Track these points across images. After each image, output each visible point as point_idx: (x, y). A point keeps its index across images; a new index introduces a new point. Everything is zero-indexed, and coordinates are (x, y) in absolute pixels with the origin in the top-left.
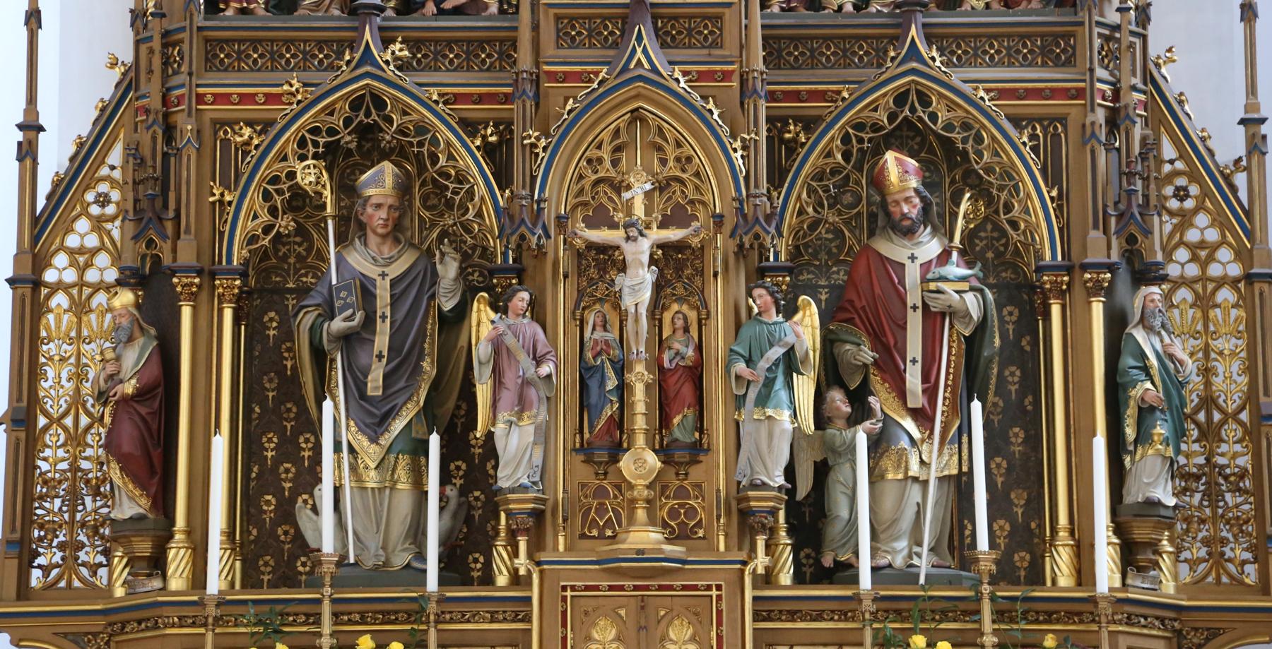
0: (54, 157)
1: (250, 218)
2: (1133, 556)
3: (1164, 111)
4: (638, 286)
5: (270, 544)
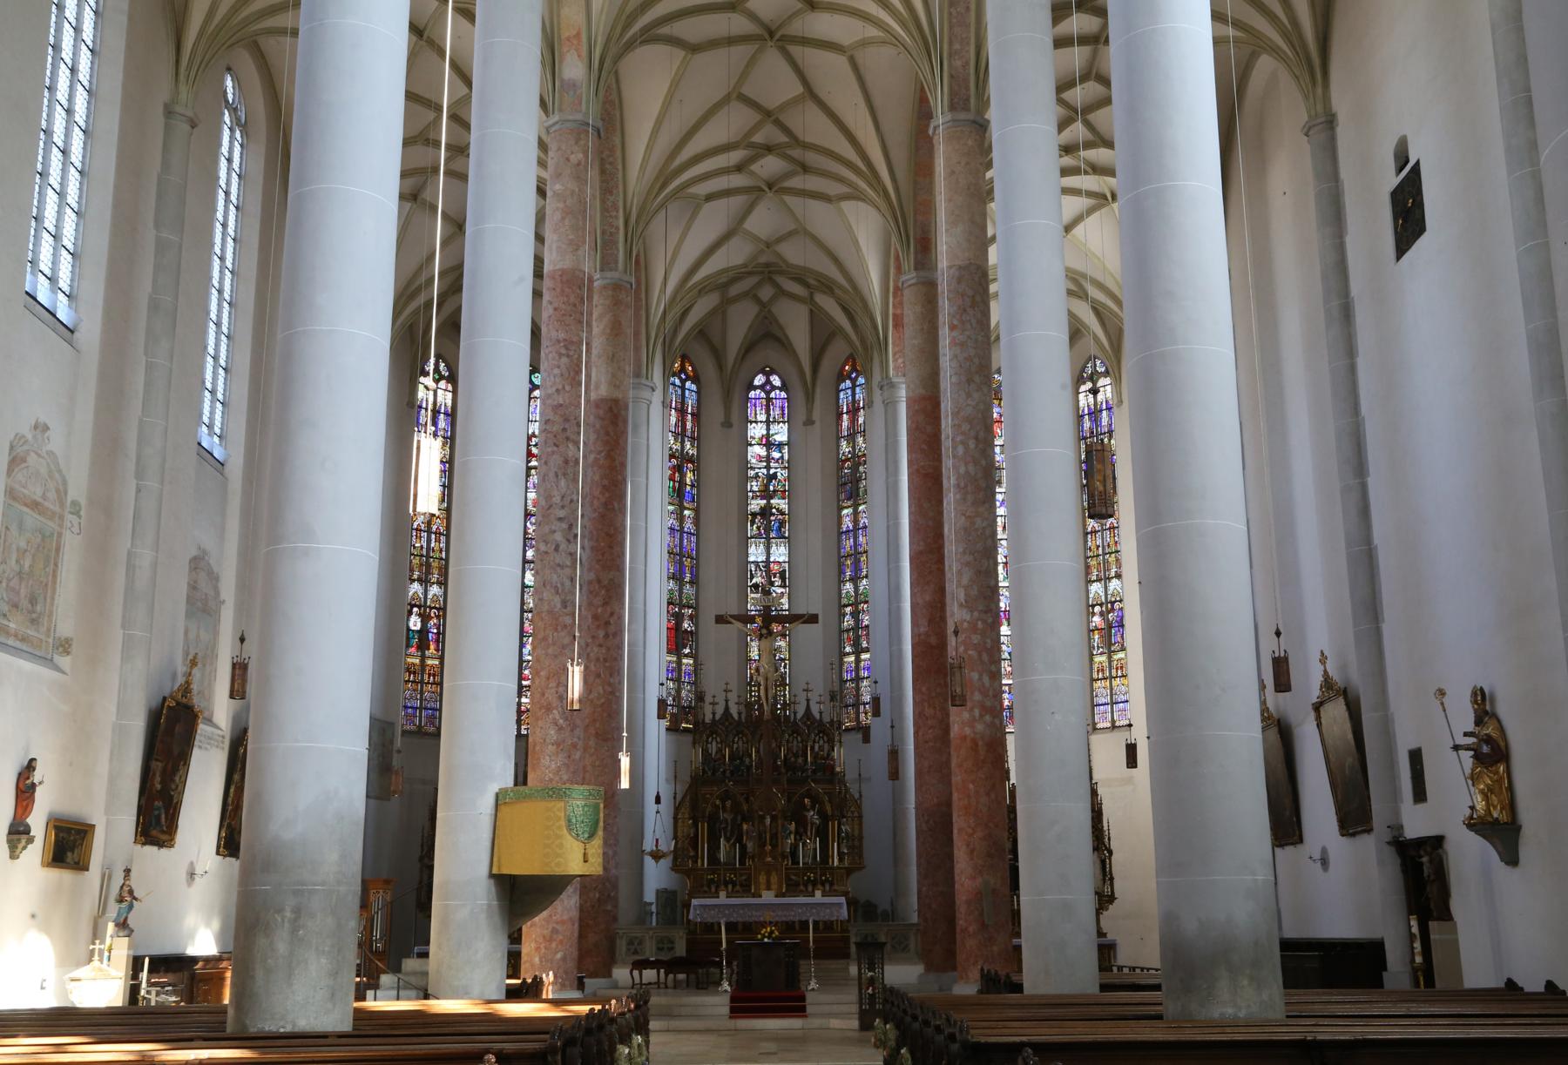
0: (679, 798)
1: (709, 809)
2: (841, 860)
3: (847, 790)
4: (768, 821)
5: (713, 859)
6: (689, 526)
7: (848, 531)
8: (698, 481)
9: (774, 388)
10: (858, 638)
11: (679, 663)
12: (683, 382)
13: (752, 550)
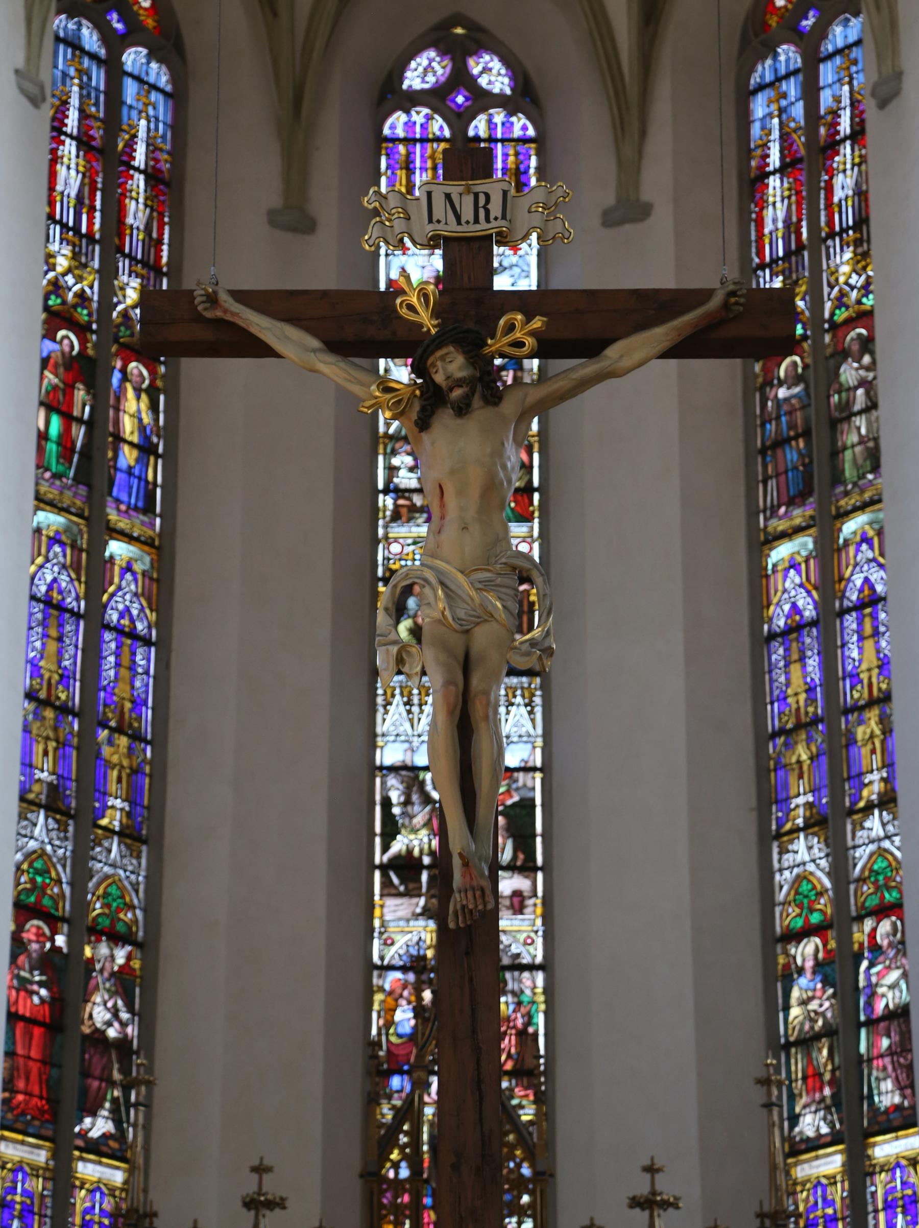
6: (124, 601)
7: (796, 628)
8: (171, 432)
9: (483, 100)
10: (853, 1070)
11: (61, 1179)
12: (115, 44)
13: (392, 719)
